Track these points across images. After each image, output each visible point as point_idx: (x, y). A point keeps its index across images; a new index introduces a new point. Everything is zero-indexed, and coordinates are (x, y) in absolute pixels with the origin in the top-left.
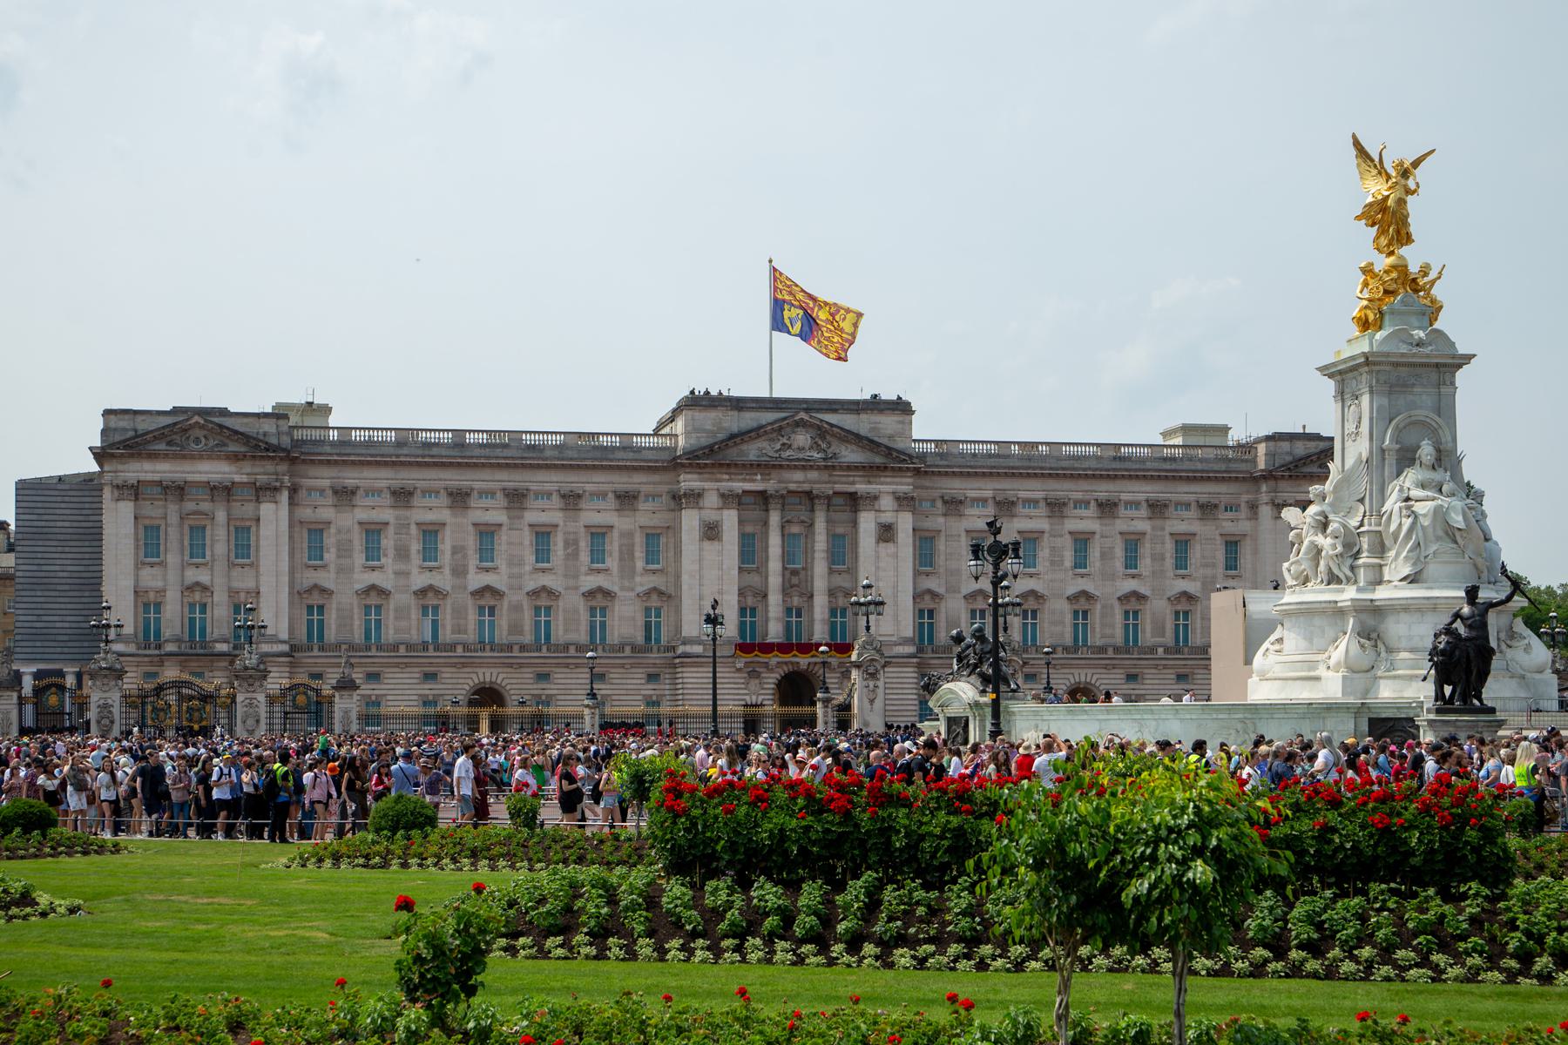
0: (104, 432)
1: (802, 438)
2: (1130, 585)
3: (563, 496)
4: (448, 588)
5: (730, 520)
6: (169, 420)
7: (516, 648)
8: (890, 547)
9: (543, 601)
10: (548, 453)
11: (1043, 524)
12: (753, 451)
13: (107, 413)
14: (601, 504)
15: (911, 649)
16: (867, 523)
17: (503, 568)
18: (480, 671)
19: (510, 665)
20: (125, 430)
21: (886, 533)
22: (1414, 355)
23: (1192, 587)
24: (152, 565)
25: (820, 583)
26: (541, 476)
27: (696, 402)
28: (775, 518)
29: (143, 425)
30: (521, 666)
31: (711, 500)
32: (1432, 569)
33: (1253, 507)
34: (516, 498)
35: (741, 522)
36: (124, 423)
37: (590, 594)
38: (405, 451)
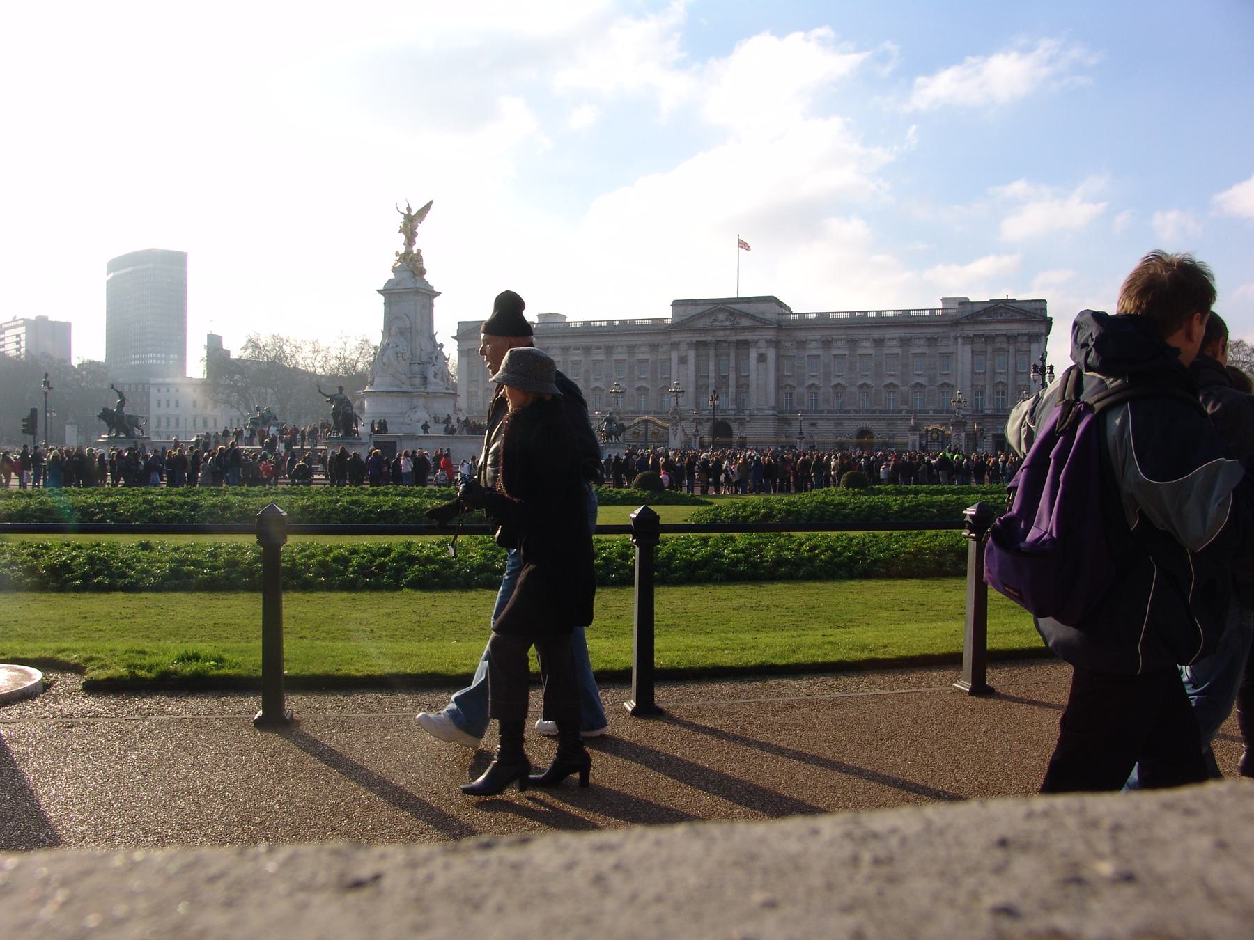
1: (722, 316)
2: (890, 380)
5: (691, 355)
8: (762, 365)
11: (846, 352)
12: (700, 324)
14: (643, 349)
15: (771, 412)
16: (753, 354)
21: (762, 358)
23: (922, 380)
25: (732, 381)
26: (619, 339)
27: (676, 304)
28: (712, 352)
31: (683, 346)
33: (956, 338)
35: (697, 356)
37: (638, 389)
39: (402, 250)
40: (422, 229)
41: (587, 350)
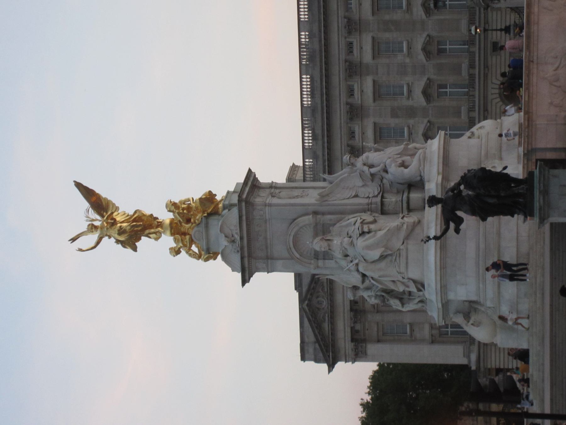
0: (317, 361)
3: (350, 33)
4: (426, 121)
6: (306, 320)
7: (471, 71)
9: (434, 48)
10: (316, 46)
13: (303, 358)
17: (409, 79)
18: (490, 97)
19: (486, 76)
20: (315, 349)
22: (242, 248)
24: (412, 330)
29: (311, 337)
30: (486, 66)
32: (414, 274)
34: (353, 69)
36: (311, 350)
38: (320, 153)
39: (168, 240)
40: (126, 205)
41: (355, 112)
